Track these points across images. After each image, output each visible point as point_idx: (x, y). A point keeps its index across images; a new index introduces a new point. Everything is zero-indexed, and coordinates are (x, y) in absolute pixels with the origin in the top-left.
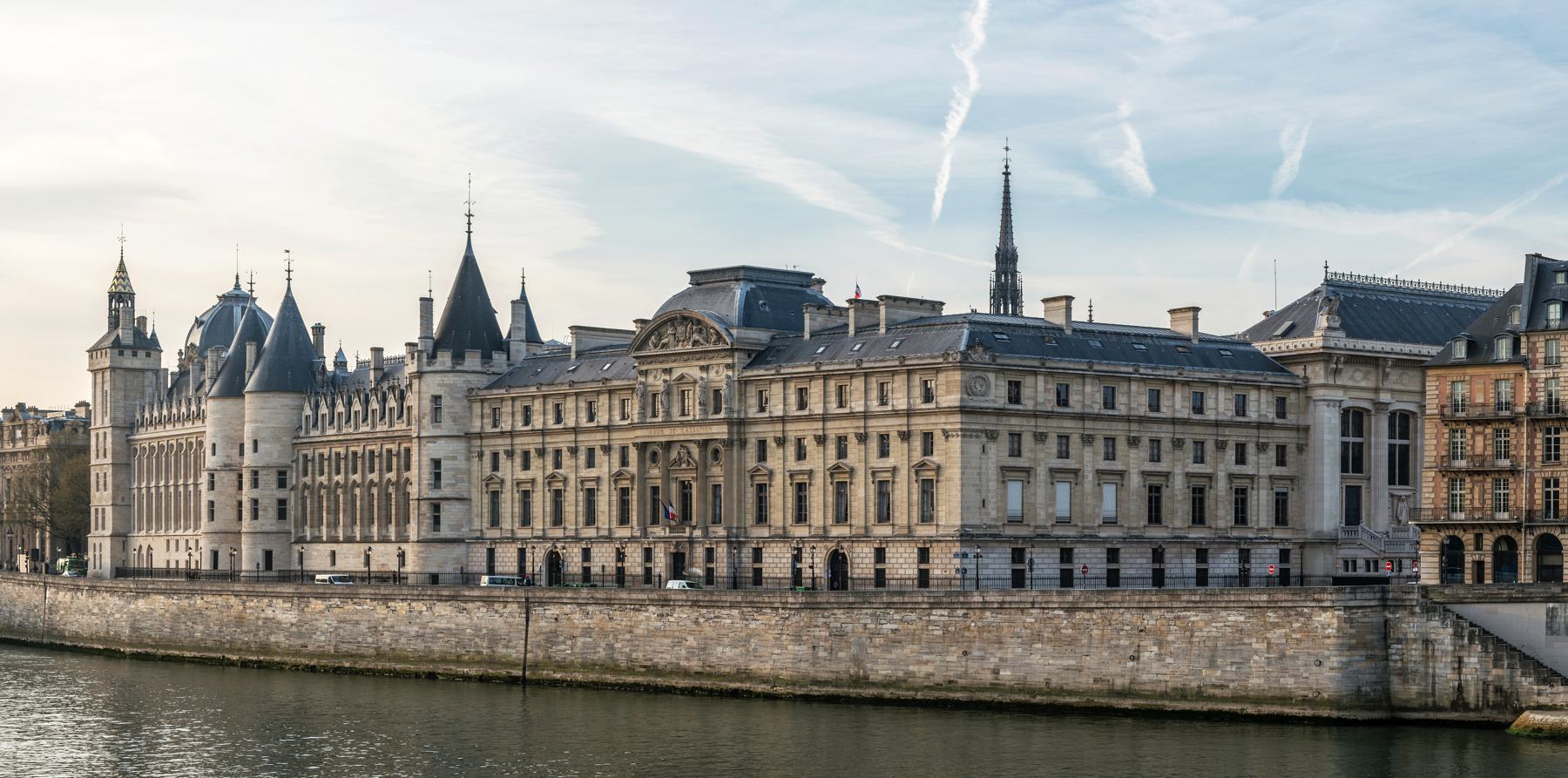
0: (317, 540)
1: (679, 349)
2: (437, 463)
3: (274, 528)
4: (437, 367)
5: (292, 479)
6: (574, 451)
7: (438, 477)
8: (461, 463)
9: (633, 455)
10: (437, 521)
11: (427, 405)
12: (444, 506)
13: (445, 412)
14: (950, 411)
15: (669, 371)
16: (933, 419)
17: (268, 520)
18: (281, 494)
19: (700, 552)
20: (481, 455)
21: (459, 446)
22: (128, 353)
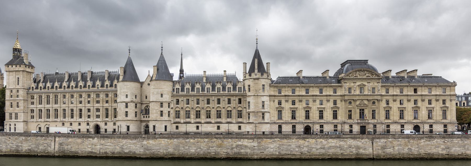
0: (190, 123)
1: (361, 77)
2: (263, 102)
3: (167, 119)
4: (264, 77)
5: (172, 106)
6: (314, 101)
7: (263, 106)
8: (268, 103)
9: (338, 102)
10: (263, 117)
11: (261, 87)
12: (266, 114)
13: (265, 89)
15: (354, 83)
16: (446, 97)
17: (165, 117)
18: (169, 110)
19: (372, 126)
20: (274, 101)
21: (268, 98)
22: (27, 67)
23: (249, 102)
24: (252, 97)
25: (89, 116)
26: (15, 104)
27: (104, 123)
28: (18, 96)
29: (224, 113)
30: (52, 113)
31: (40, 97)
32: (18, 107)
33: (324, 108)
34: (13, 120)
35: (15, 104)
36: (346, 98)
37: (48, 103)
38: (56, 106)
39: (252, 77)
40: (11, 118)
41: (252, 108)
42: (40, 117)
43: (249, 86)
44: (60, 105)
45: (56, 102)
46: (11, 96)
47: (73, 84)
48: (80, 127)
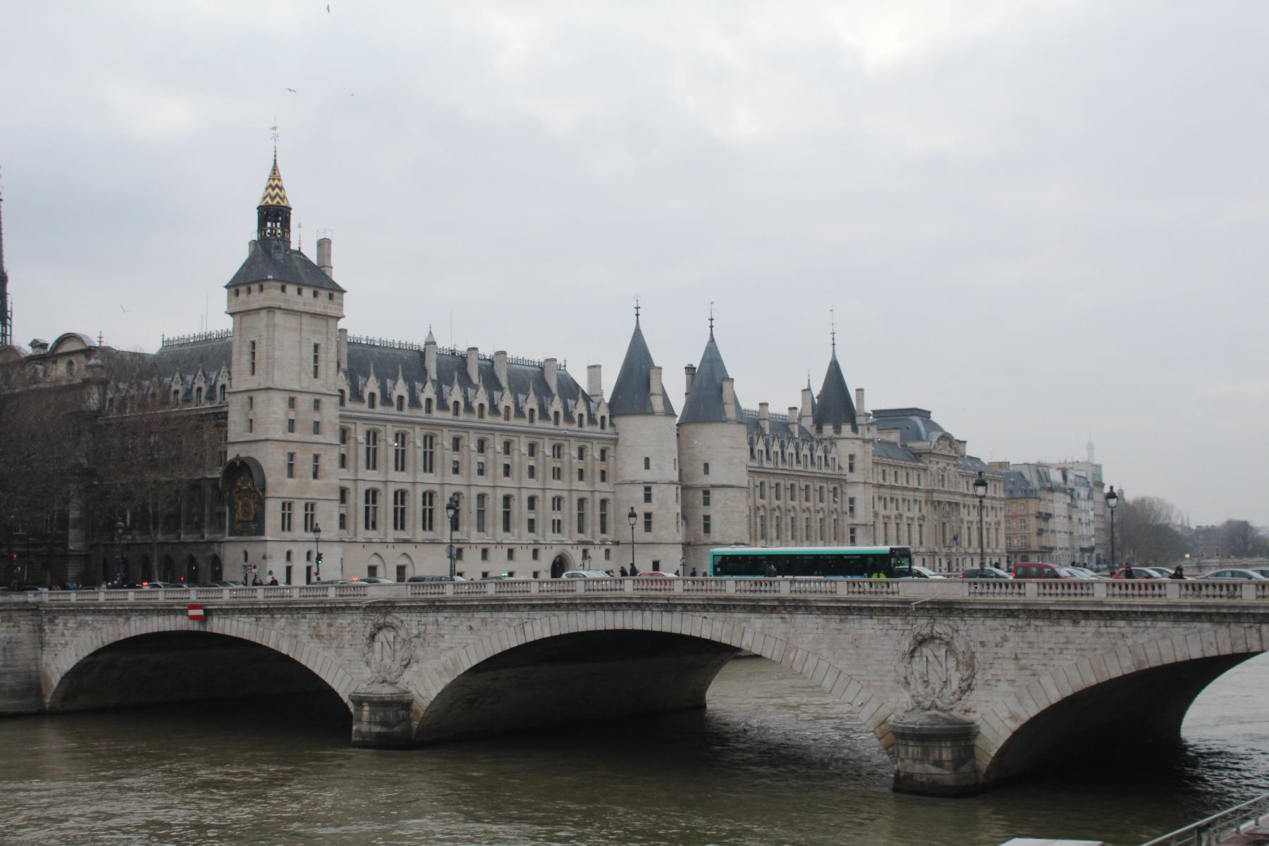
14: (1001, 499)
23: (852, 500)
24: (861, 486)
25: (532, 525)
26: (304, 463)
27: (581, 548)
28: (317, 427)
29: (816, 526)
30: (415, 507)
31: (372, 436)
32: (315, 476)
33: (912, 519)
34: (298, 531)
35: (304, 463)
36: (936, 497)
37: (400, 465)
38: (430, 480)
39: (859, 436)
40: (287, 524)
41: (862, 514)
42: (371, 523)
43: (852, 457)
44: (443, 474)
45: (429, 467)
46: (291, 426)
47: (455, 394)
48: (512, 566)
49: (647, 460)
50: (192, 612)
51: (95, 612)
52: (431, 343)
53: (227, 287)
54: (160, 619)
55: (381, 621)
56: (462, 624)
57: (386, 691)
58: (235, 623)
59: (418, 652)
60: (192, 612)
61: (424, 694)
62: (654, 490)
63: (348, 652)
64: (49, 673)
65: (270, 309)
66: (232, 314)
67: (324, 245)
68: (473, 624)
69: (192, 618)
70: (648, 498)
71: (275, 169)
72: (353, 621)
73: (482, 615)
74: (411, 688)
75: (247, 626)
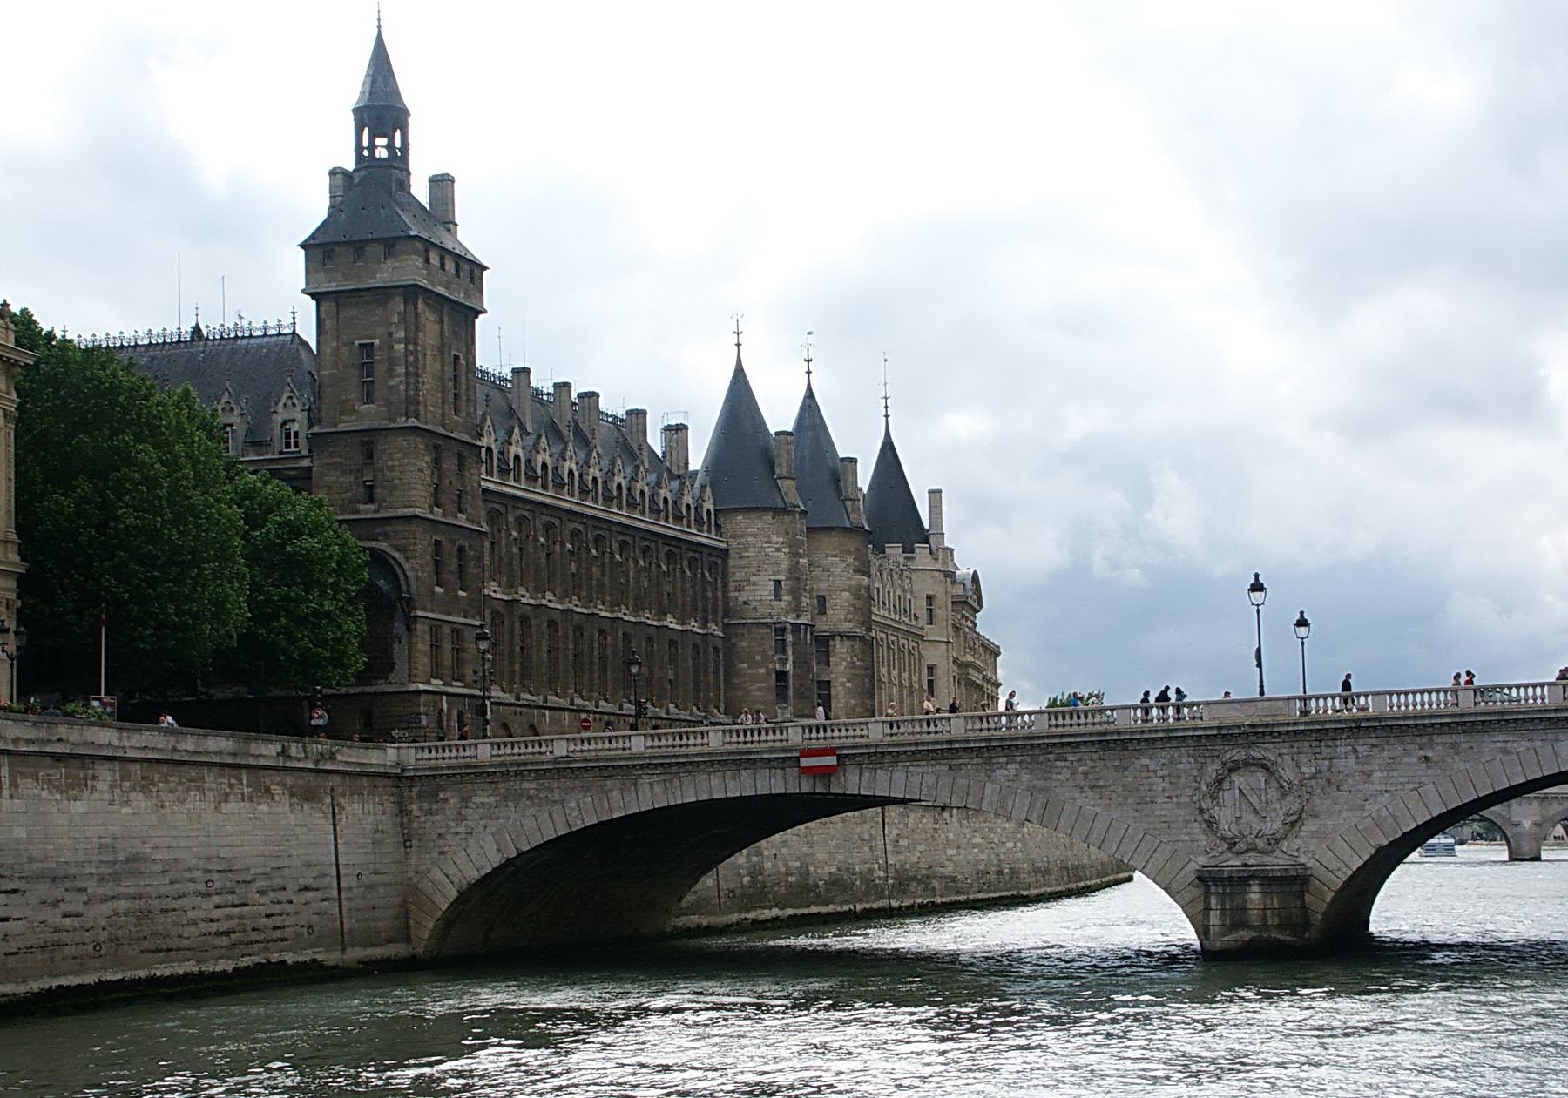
39: (939, 566)
49: (778, 582)
50: (805, 762)
51: (540, 774)
52: (522, 373)
53: (303, 246)
54: (716, 780)
55: (1238, 754)
56: (1408, 754)
57: (1276, 861)
58: (899, 775)
59: (1317, 801)
60: (805, 762)
61: (1334, 865)
62: (790, 638)
63: (1162, 809)
64: (426, 886)
65: (412, 292)
66: (313, 296)
67: (442, 185)
68: (1430, 754)
69: (807, 770)
70: (781, 646)
71: (380, 42)
72: (1172, 760)
73: (1449, 739)
74: (1303, 859)
75: (930, 780)
